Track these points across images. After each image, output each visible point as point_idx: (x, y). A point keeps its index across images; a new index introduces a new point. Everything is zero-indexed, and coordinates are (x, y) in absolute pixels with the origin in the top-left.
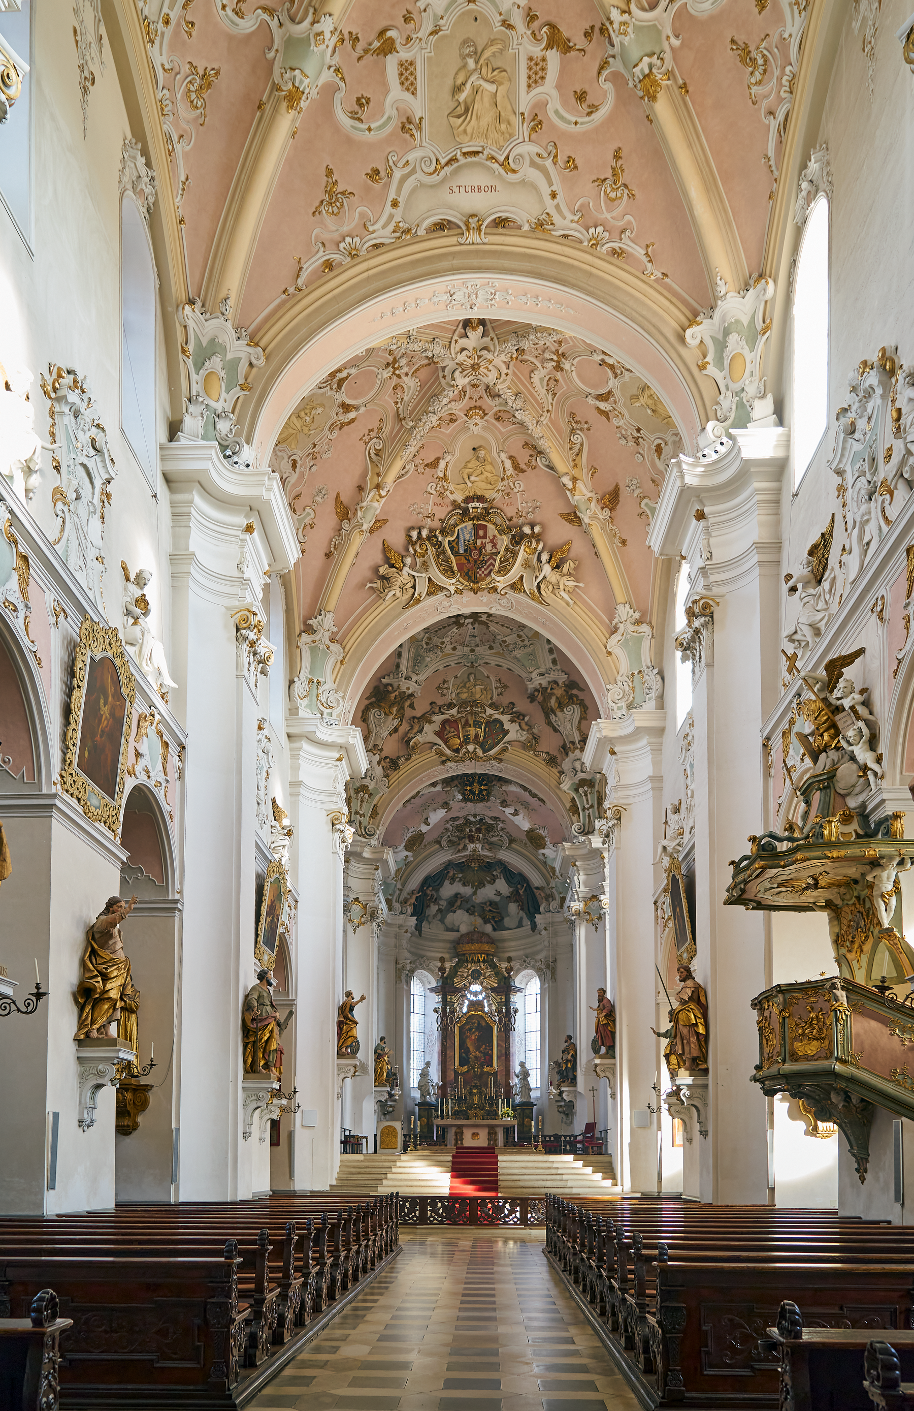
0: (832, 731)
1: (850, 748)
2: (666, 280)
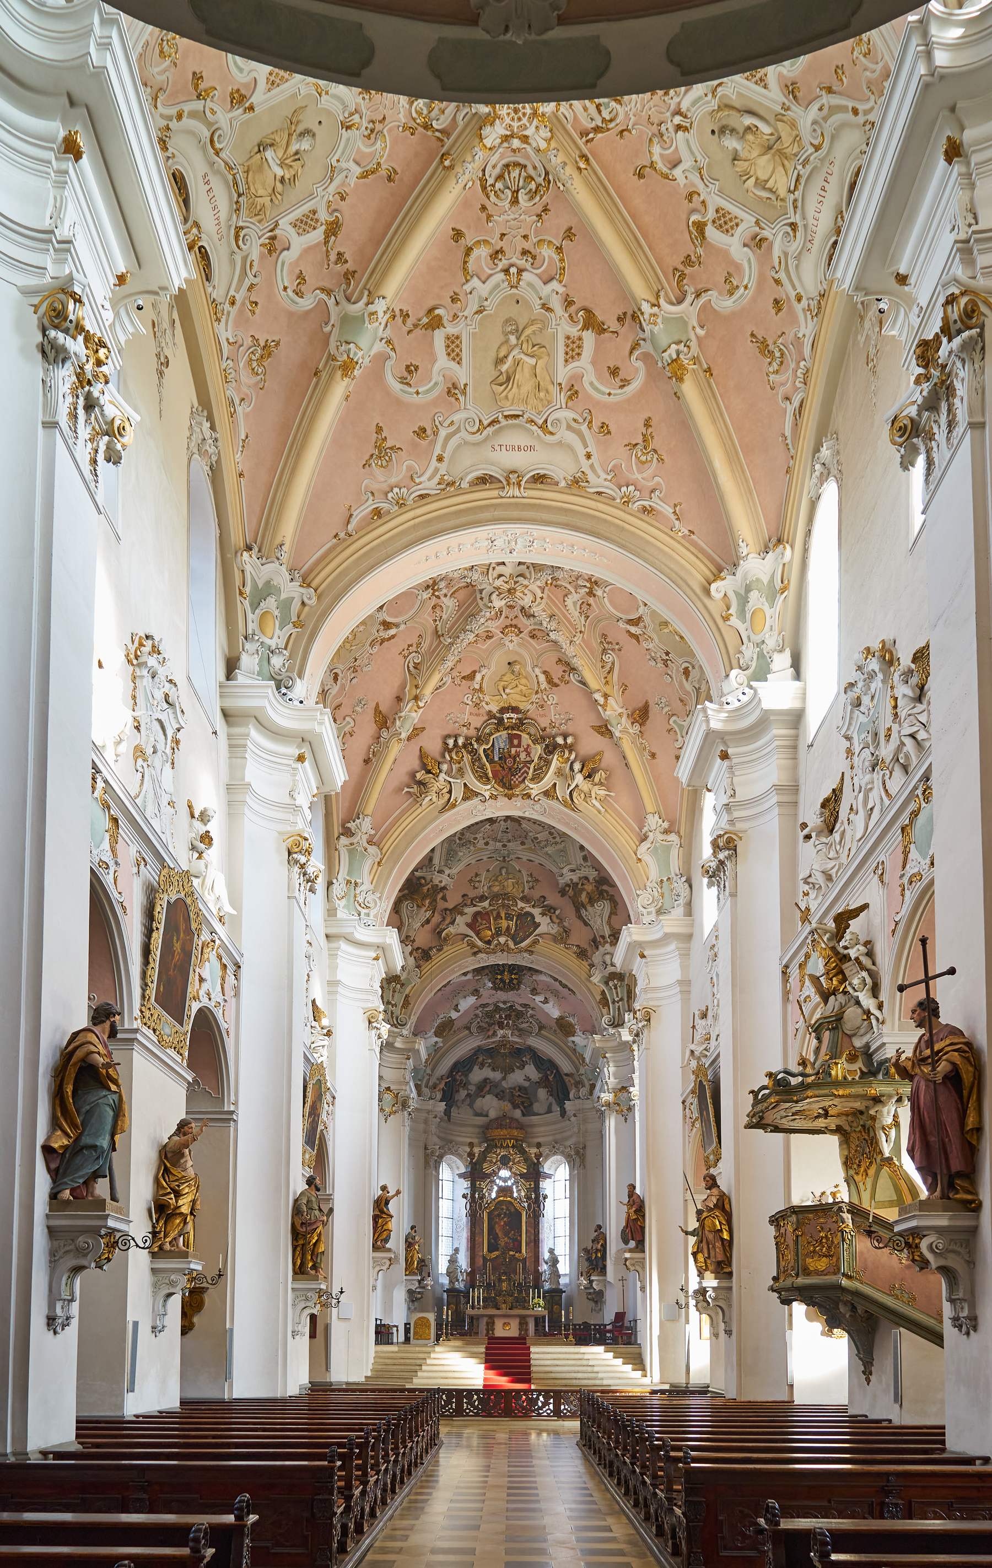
0: (840, 977)
1: (856, 994)
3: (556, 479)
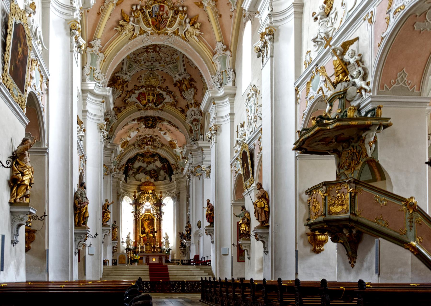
0: (344, 74)
1: (353, 80)
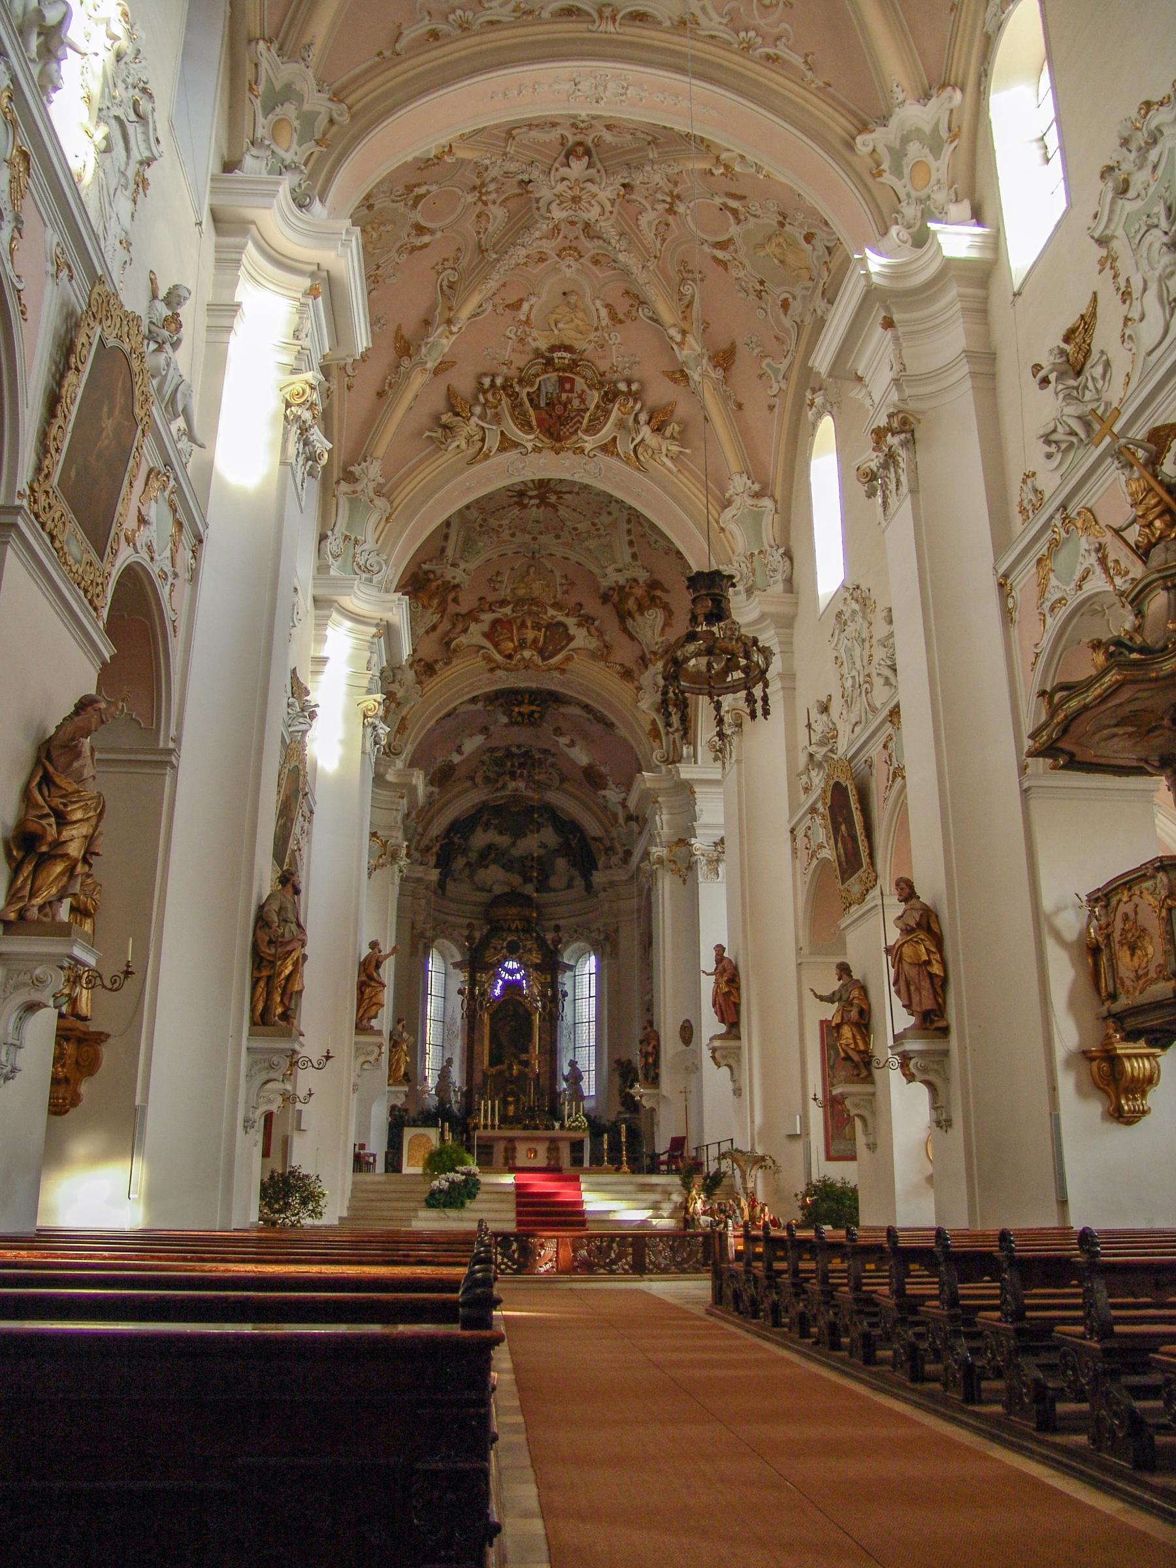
2: (829, 89)
3: (660, 17)
